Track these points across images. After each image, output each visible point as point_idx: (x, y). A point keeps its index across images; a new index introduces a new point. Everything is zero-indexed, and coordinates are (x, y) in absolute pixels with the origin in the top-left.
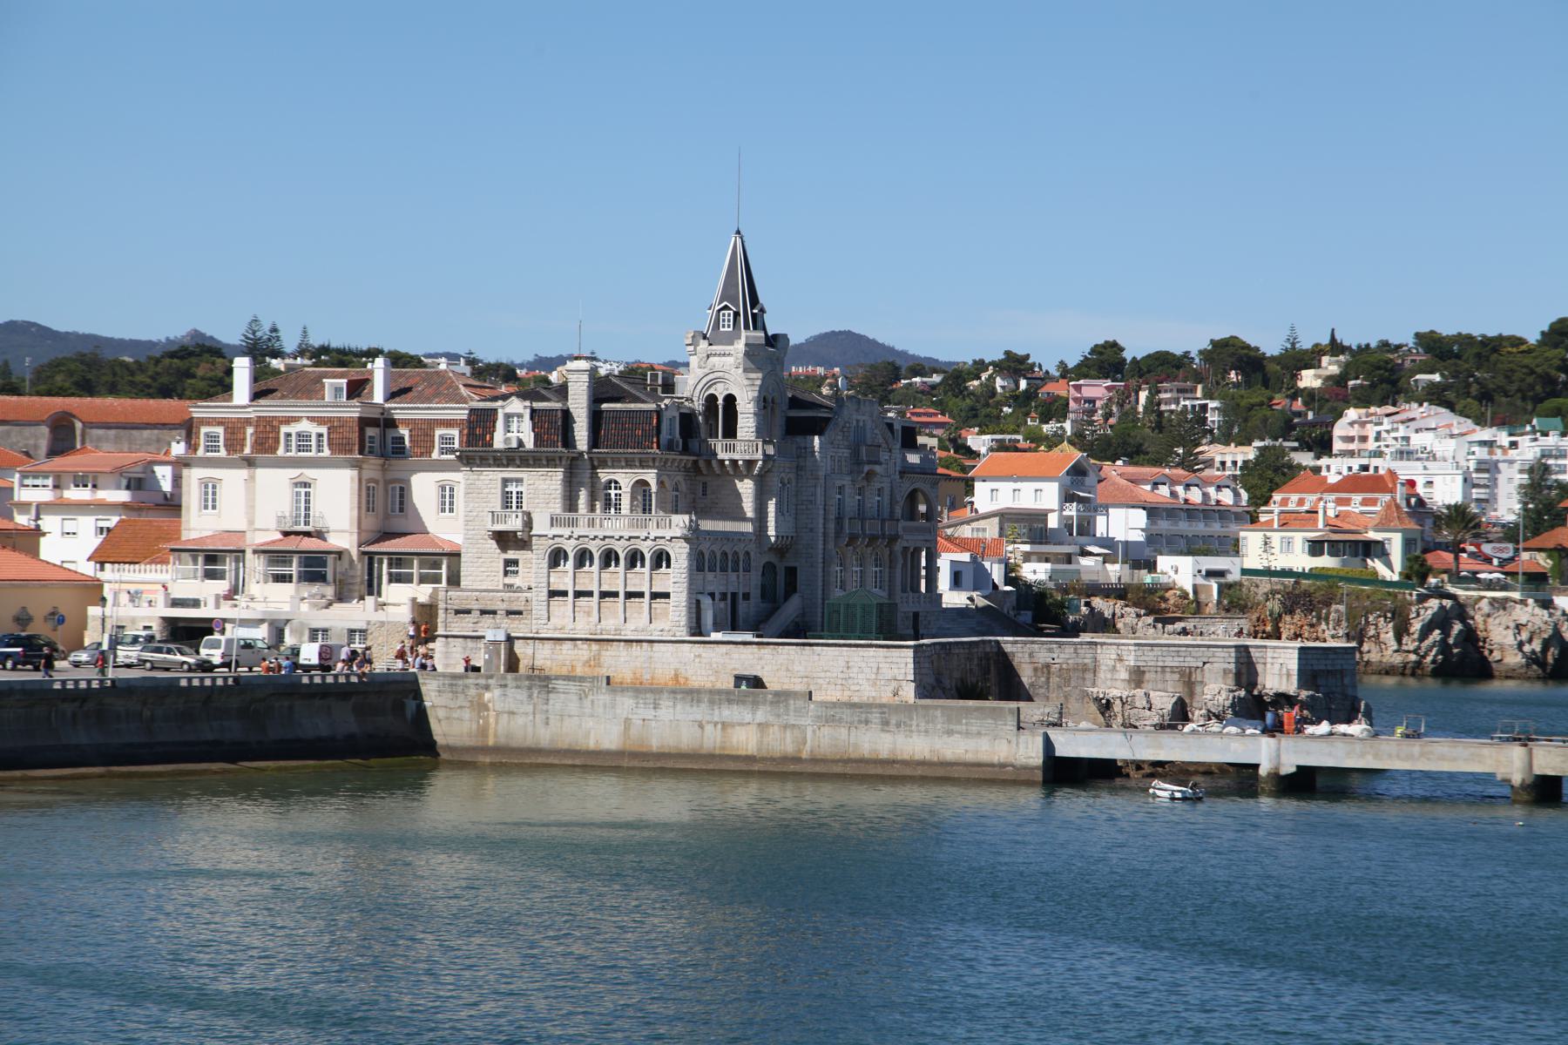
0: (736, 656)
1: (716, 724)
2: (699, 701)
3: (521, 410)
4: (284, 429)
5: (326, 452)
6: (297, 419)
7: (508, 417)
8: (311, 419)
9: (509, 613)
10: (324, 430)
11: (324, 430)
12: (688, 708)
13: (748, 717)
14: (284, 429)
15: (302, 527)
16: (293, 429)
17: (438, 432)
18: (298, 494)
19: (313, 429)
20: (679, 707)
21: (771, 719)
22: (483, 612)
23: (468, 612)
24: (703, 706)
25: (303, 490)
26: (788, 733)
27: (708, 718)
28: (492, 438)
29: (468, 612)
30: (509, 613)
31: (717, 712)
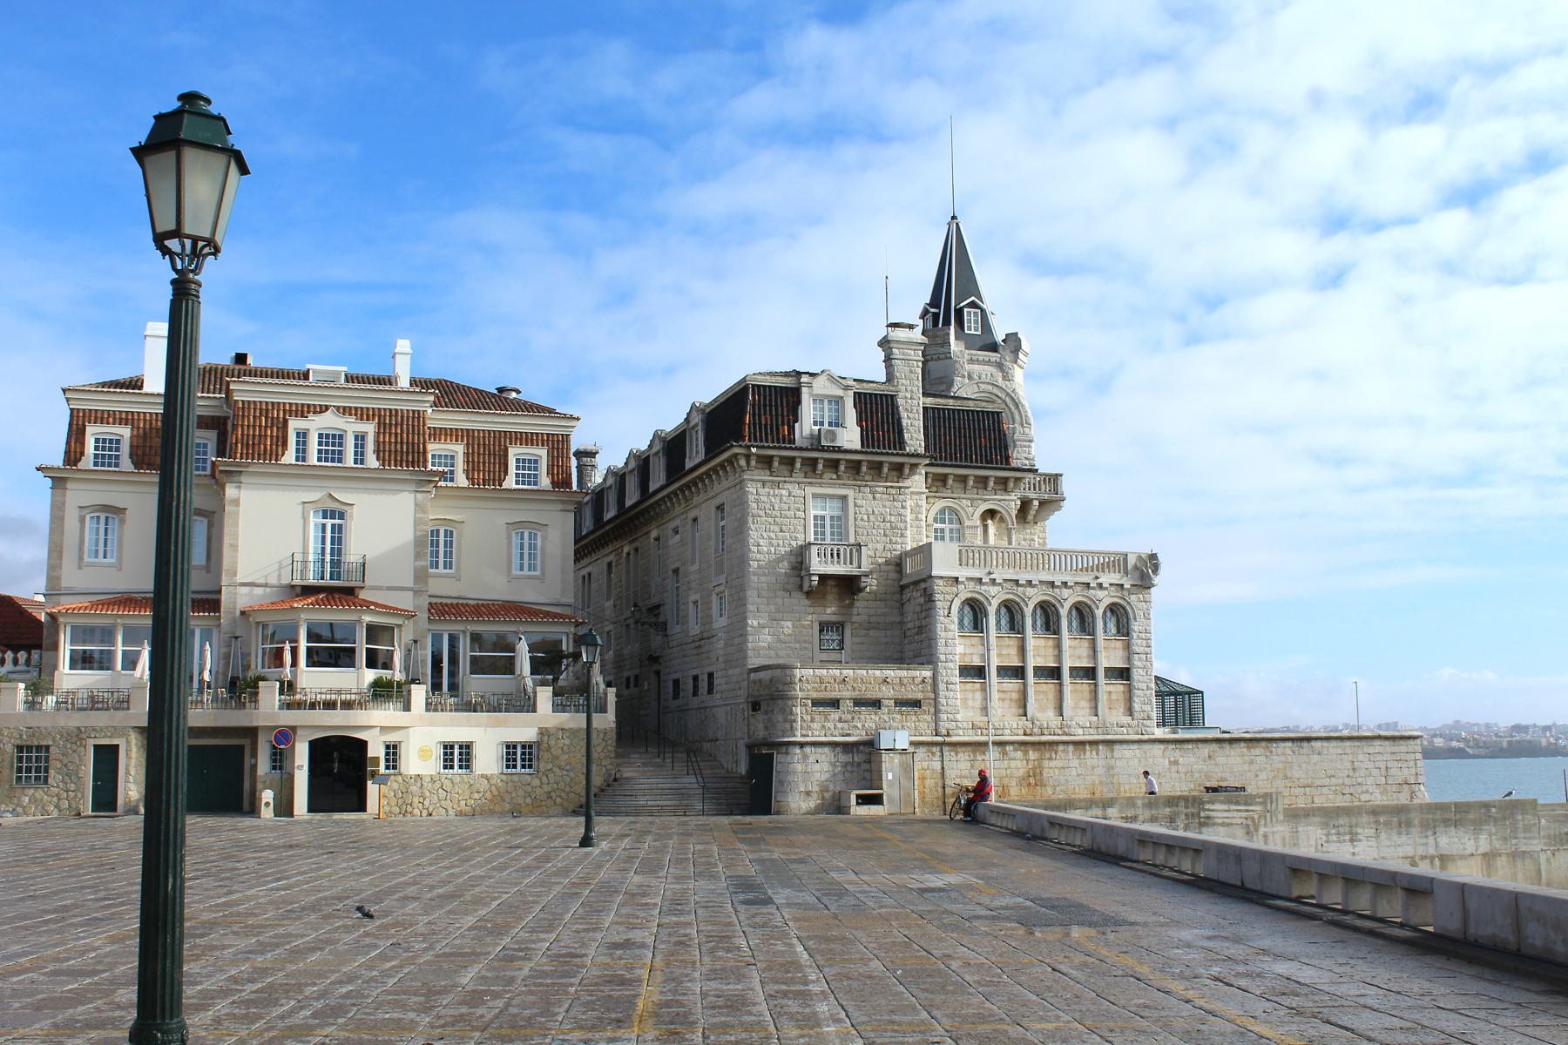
0: (1221, 760)
1: (1432, 858)
2: (1409, 824)
3: (840, 393)
4: (294, 424)
5: (372, 461)
6: (323, 409)
7: (819, 399)
8: (346, 411)
9: (900, 703)
10: (370, 428)
11: (370, 428)
12: (1395, 837)
13: (1470, 846)
14: (294, 424)
15: (327, 582)
16: (315, 425)
17: (514, 452)
18: (324, 526)
19: (351, 427)
20: (1383, 836)
21: (1497, 844)
22: (858, 703)
23: (835, 703)
24: (1415, 831)
25: (329, 522)
26: (1519, 863)
27: (1421, 851)
28: (792, 430)
29: (835, 703)
30: (900, 703)
31: (1431, 840)
